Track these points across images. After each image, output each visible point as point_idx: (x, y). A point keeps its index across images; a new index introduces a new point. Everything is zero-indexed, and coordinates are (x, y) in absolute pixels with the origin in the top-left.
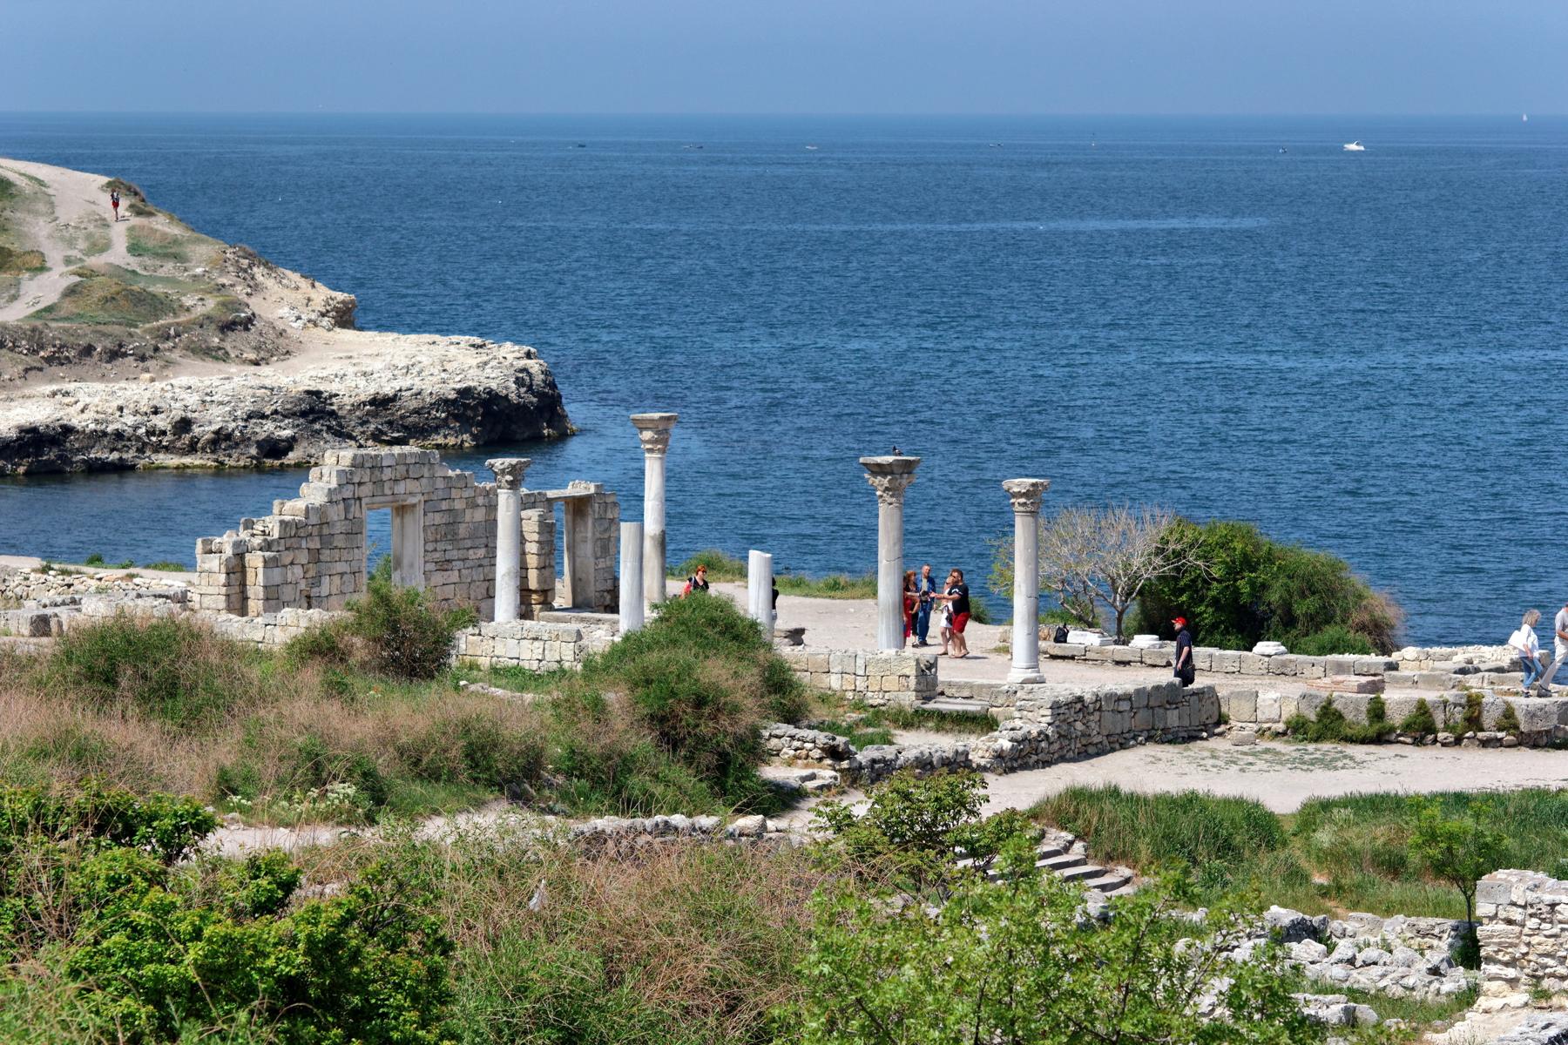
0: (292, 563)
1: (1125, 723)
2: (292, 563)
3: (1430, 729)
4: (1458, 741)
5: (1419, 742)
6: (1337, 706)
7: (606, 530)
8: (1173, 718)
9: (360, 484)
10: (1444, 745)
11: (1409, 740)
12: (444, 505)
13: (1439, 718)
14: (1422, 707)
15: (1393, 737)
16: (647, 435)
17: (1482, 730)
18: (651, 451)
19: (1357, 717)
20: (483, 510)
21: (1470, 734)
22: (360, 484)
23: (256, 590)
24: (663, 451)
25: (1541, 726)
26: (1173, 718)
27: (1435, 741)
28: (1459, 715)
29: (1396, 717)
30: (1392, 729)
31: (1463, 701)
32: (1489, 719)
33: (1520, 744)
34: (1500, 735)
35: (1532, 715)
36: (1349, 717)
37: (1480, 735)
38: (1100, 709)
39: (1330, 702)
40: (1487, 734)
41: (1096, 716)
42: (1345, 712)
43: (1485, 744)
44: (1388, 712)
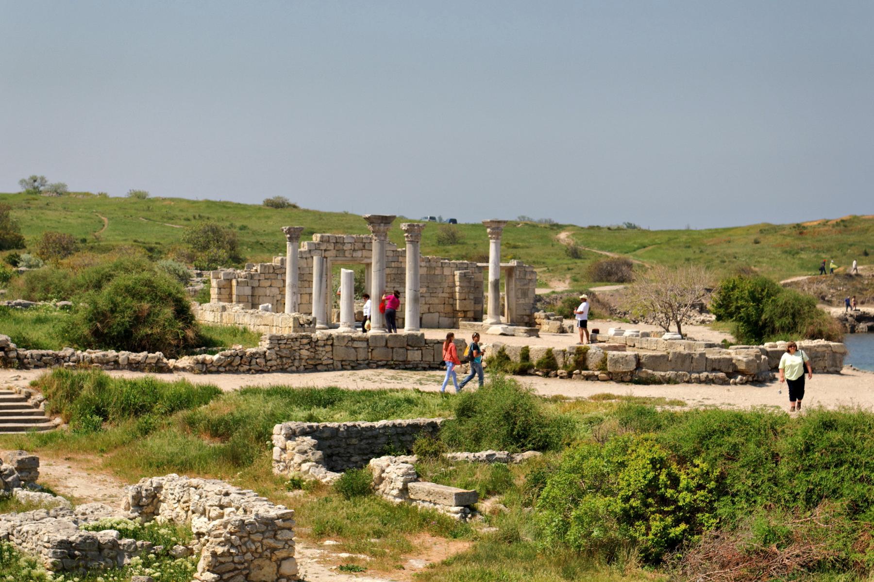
0: (271, 286)
1: (377, 354)
2: (271, 286)
3: (554, 367)
4: (570, 376)
5: (547, 375)
6: (507, 352)
7: (525, 285)
8: (414, 356)
9: (325, 250)
10: (561, 378)
11: (540, 374)
12: (393, 265)
13: (560, 361)
14: (549, 352)
15: (532, 371)
16: (489, 230)
17: (587, 369)
18: (491, 238)
19: (516, 359)
20: (425, 269)
21: (577, 371)
22: (325, 250)
23: (234, 297)
24: (497, 239)
25: (622, 368)
26: (414, 356)
27: (556, 376)
28: (571, 360)
29: (535, 359)
30: (531, 367)
31: (574, 351)
32: (593, 361)
33: (611, 379)
34: (596, 373)
35: (616, 361)
36: (512, 358)
37: (583, 372)
38: (332, 345)
39: (503, 349)
40: (591, 372)
41: (328, 348)
42: (510, 355)
43: (587, 378)
44: (531, 356)
